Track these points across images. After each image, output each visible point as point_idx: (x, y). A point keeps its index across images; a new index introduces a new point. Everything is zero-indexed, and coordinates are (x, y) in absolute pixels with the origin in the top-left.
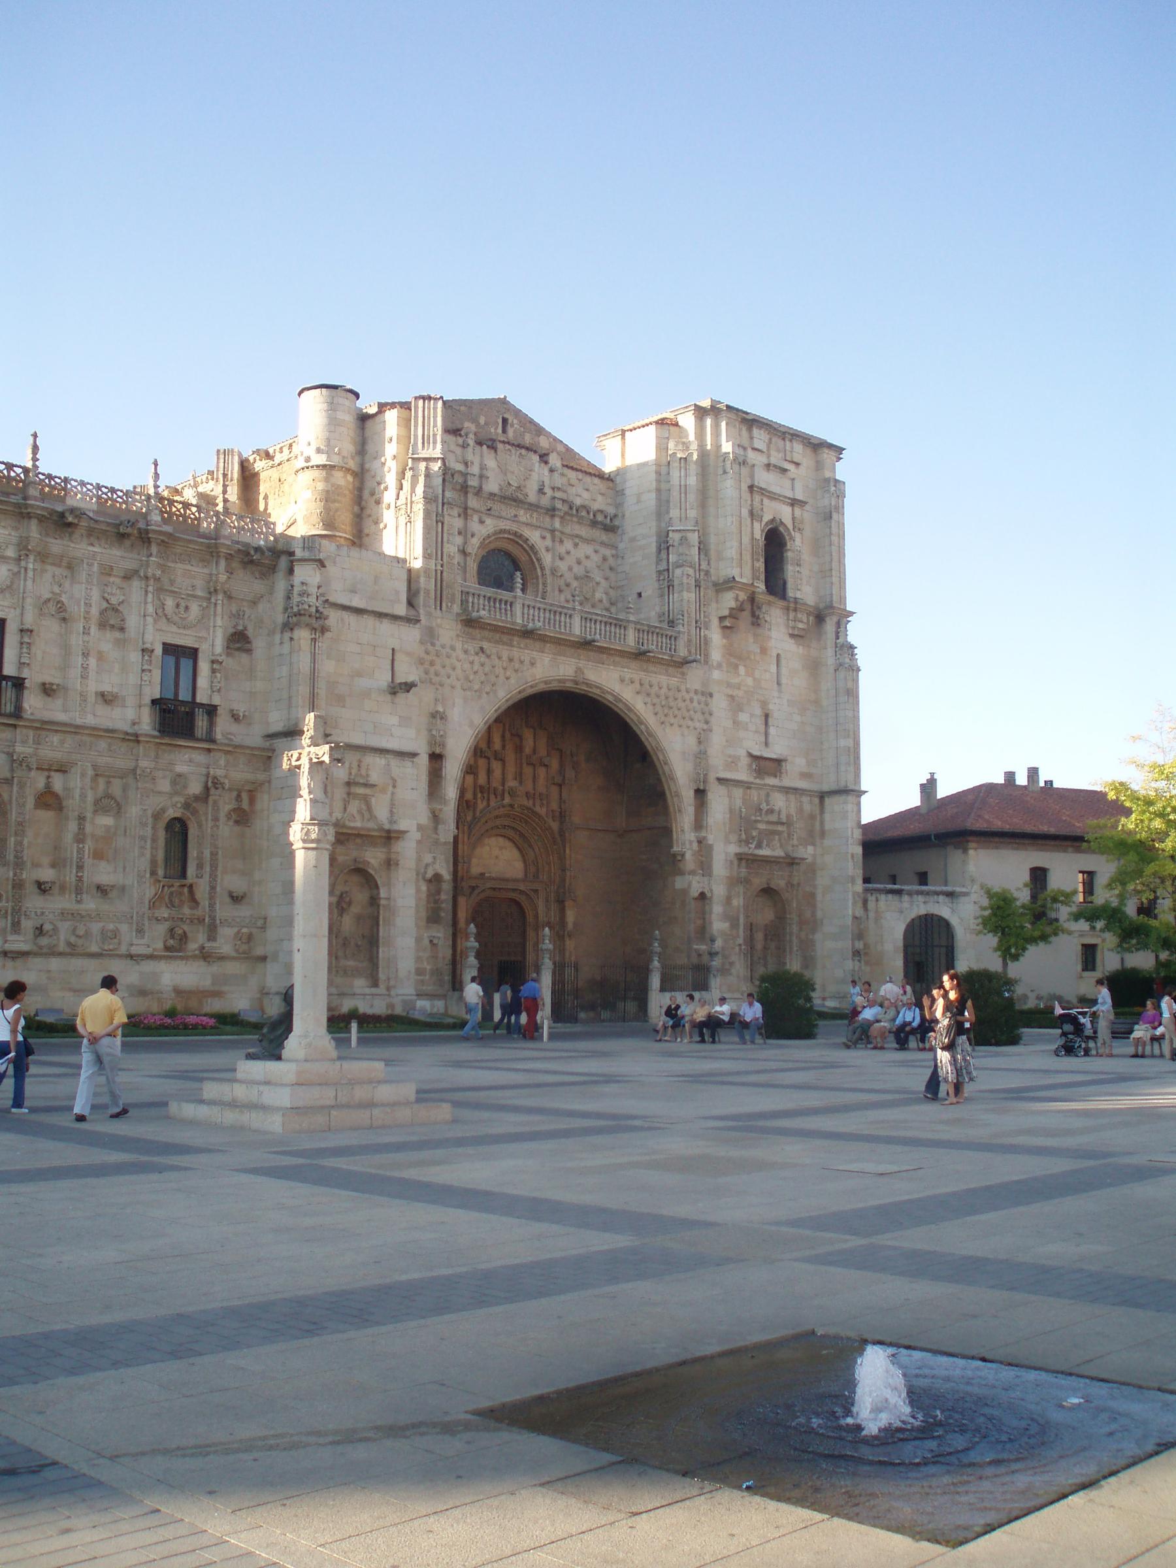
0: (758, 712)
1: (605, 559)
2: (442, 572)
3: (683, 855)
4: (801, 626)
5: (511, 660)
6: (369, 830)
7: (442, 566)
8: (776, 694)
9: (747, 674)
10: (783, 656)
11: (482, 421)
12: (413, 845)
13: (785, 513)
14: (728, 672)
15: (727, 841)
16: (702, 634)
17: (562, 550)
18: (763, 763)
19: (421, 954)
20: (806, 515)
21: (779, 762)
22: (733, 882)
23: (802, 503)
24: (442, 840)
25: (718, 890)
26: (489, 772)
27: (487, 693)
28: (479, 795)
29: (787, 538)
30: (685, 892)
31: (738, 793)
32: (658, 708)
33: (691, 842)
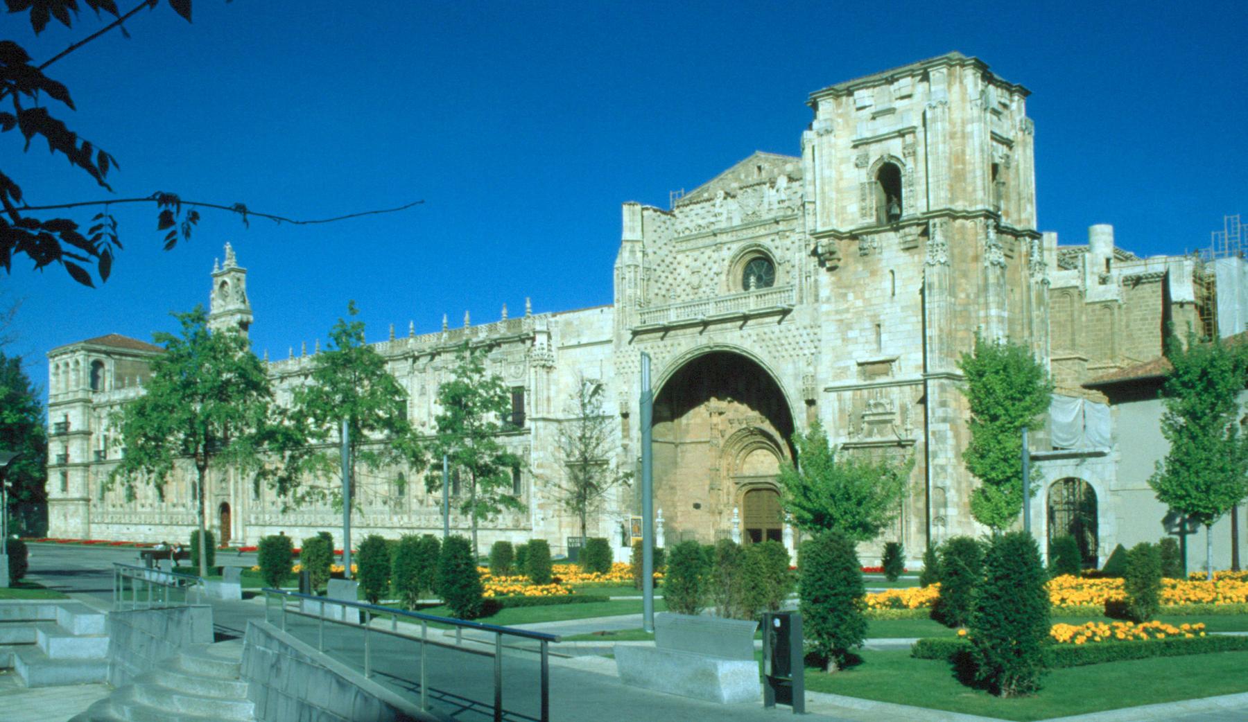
0: (868, 324)
4: (910, 238)
9: (856, 298)
13: (895, 148)
14: (836, 302)
21: (889, 361)
29: (899, 165)
32: (772, 349)
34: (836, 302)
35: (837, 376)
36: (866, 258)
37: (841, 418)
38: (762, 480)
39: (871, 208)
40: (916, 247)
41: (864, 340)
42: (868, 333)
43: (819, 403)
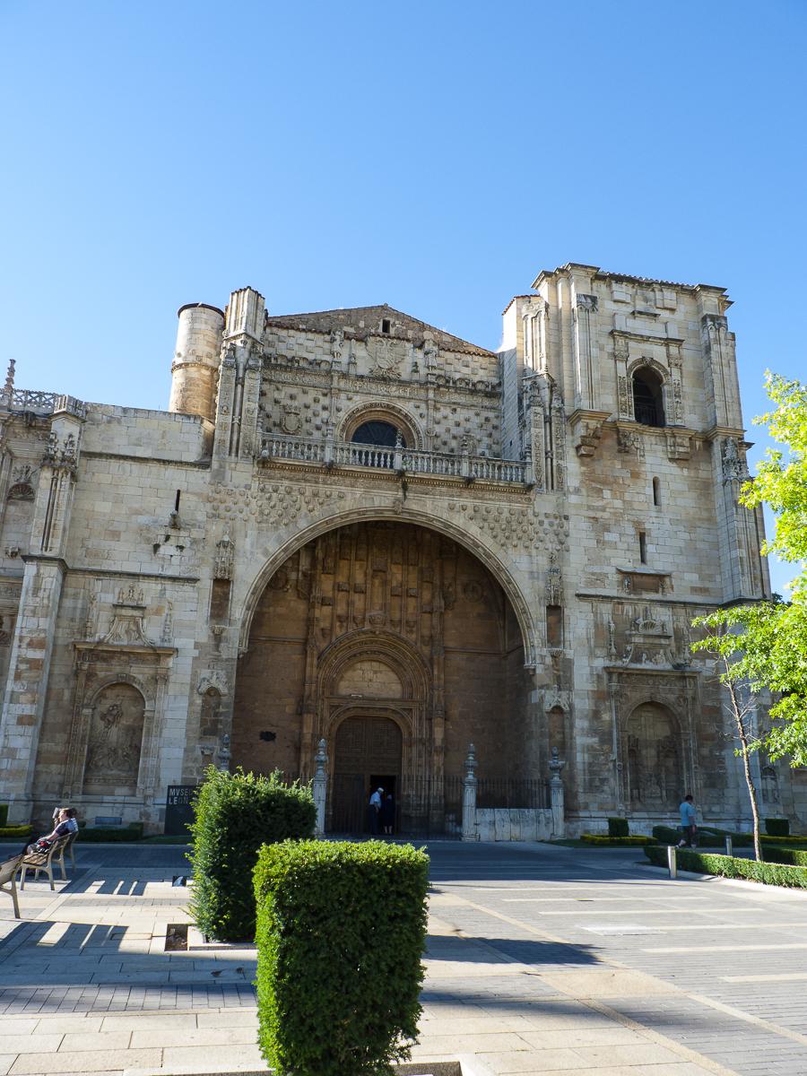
0: (631, 530)
1: (487, 419)
2: (240, 425)
3: (534, 670)
4: (681, 449)
5: (315, 495)
6: (134, 647)
7: (240, 420)
8: (654, 514)
10: (661, 478)
11: (362, 324)
12: (190, 661)
13: (658, 353)
14: (588, 496)
15: (592, 655)
16: (555, 463)
17: (438, 416)
18: (636, 579)
19: (190, 764)
20: (688, 354)
22: (600, 697)
23: (679, 342)
24: (224, 657)
25: (582, 704)
26: (349, 604)
27: (286, 525)
28: (338, 624)
30: (539, 706)
31: (606, 609)
33: (543, 657)
34: (588, 496)
35: (590, 583)
36: (628, 458)
37: (597, 635)
38: (378, 705)
39: (630, 406)
40: (686, 460)
41: (625, 546)
42: (631, 540)
43: (567, 612)
